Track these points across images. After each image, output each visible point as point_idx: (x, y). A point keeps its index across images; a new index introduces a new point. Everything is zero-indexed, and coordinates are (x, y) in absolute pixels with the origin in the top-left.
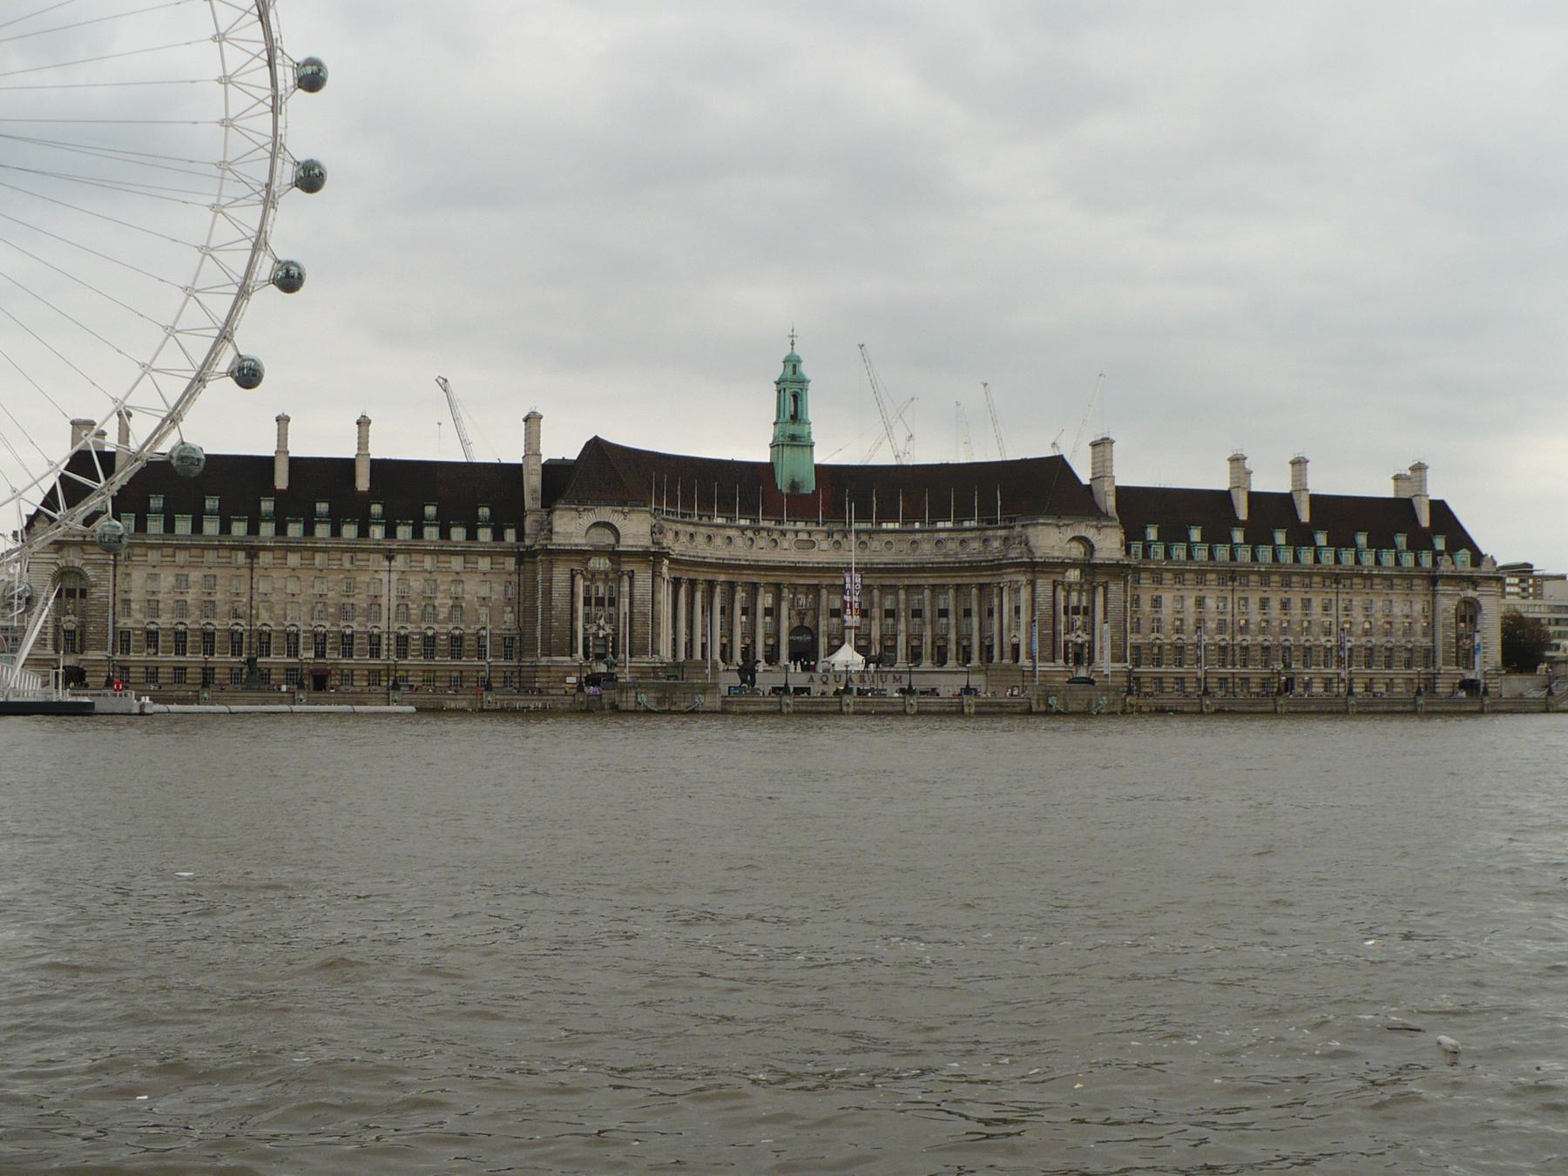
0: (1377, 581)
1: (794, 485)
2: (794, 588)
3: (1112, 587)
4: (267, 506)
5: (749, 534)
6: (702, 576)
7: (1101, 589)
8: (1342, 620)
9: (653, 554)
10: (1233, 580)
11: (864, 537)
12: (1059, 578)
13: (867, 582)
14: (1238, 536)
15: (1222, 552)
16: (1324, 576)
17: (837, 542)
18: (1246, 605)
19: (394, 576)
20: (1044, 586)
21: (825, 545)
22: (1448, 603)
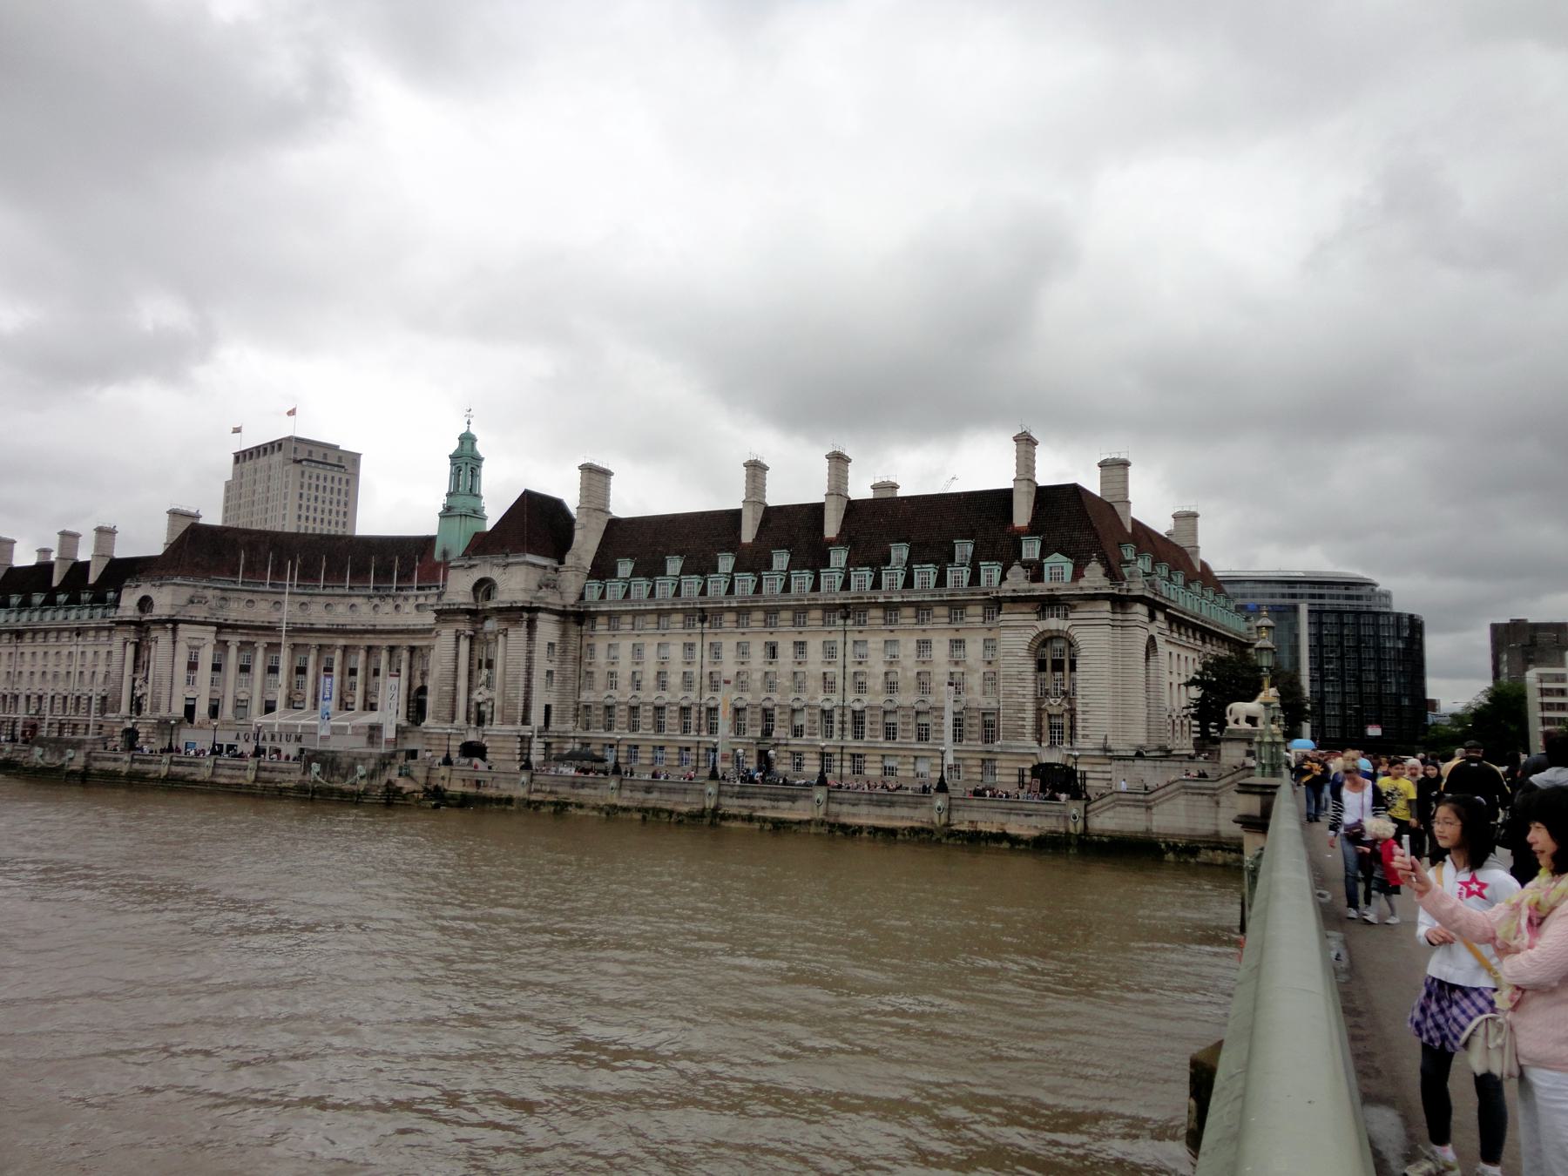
0: (909, 612)
1: (445, 554)
2: (412, 650)
3: (512, 634)
4: (38, 599)
5: (376, 601)
6: (314, 641)
7: (501, 637)
8: (851, 670)
9: (168, 621)
10: (703, 620)
12: (461, 627)
14: (726, 563)
15: (692, 584)
16: (828, 609)
18: (717, 655)
19: (80, 649)
22: (1017, 636)
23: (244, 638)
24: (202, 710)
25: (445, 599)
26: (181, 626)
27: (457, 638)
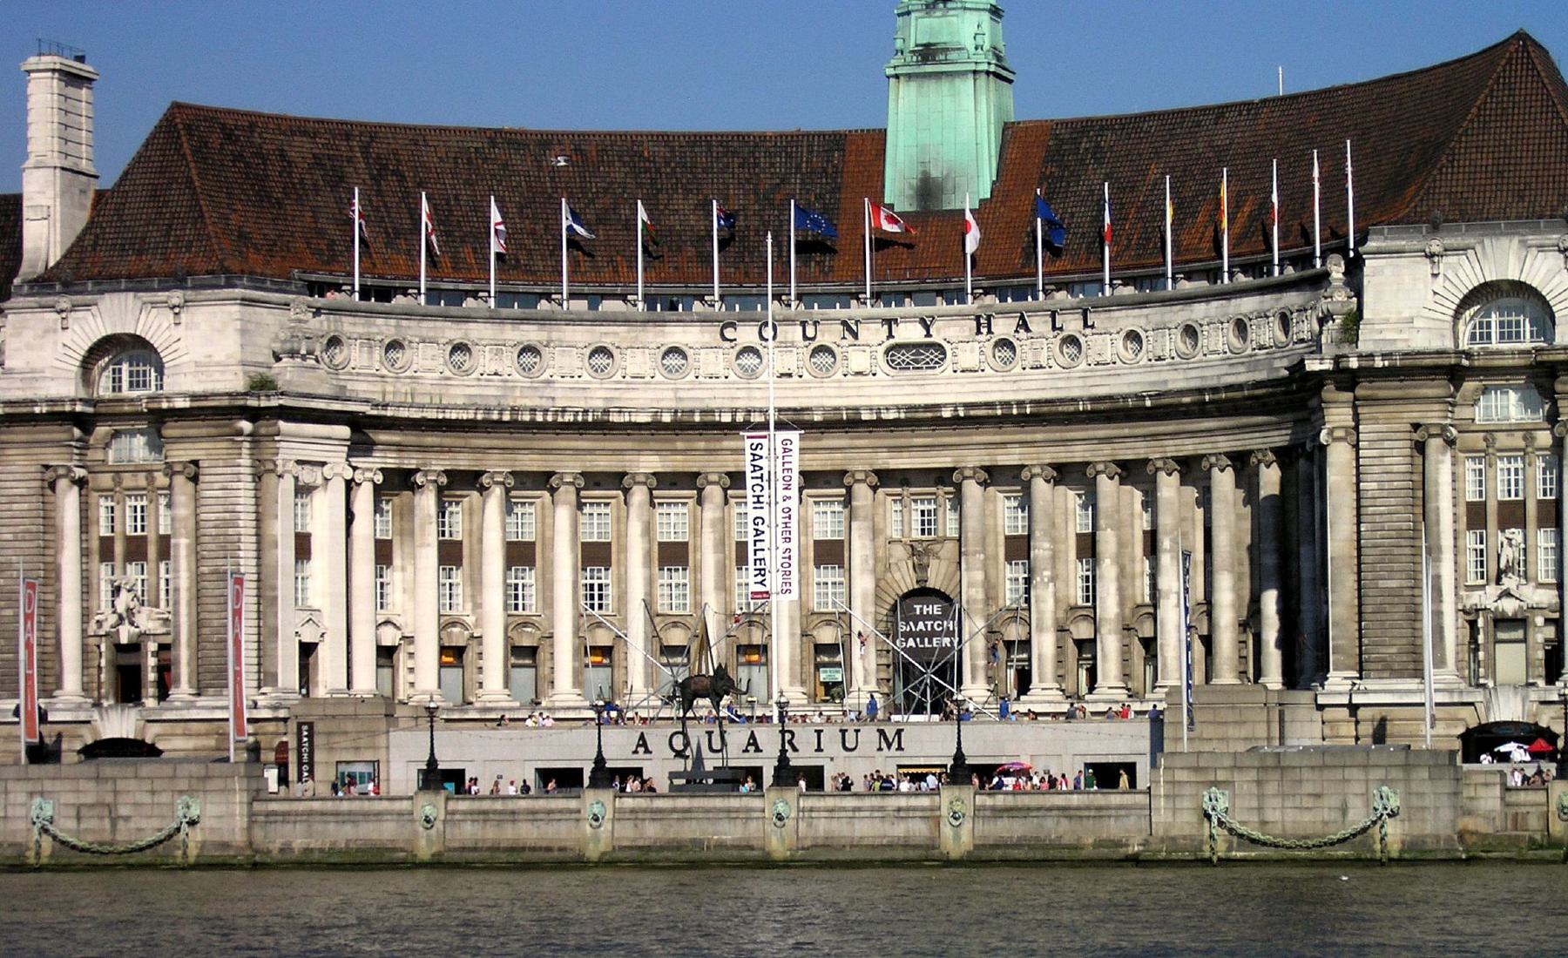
1: (928, 189)
6: (570, 461)
11: (1072, 325)
12: (1432, 415)
13: (818, 462)
17: (1004, 343)
20: (1384, 439)
21: (969, 355)
23: (392, 461)
24: (329, 677)
25: (1368, 340)
26: (283, 425)
27: (1420, 447)
